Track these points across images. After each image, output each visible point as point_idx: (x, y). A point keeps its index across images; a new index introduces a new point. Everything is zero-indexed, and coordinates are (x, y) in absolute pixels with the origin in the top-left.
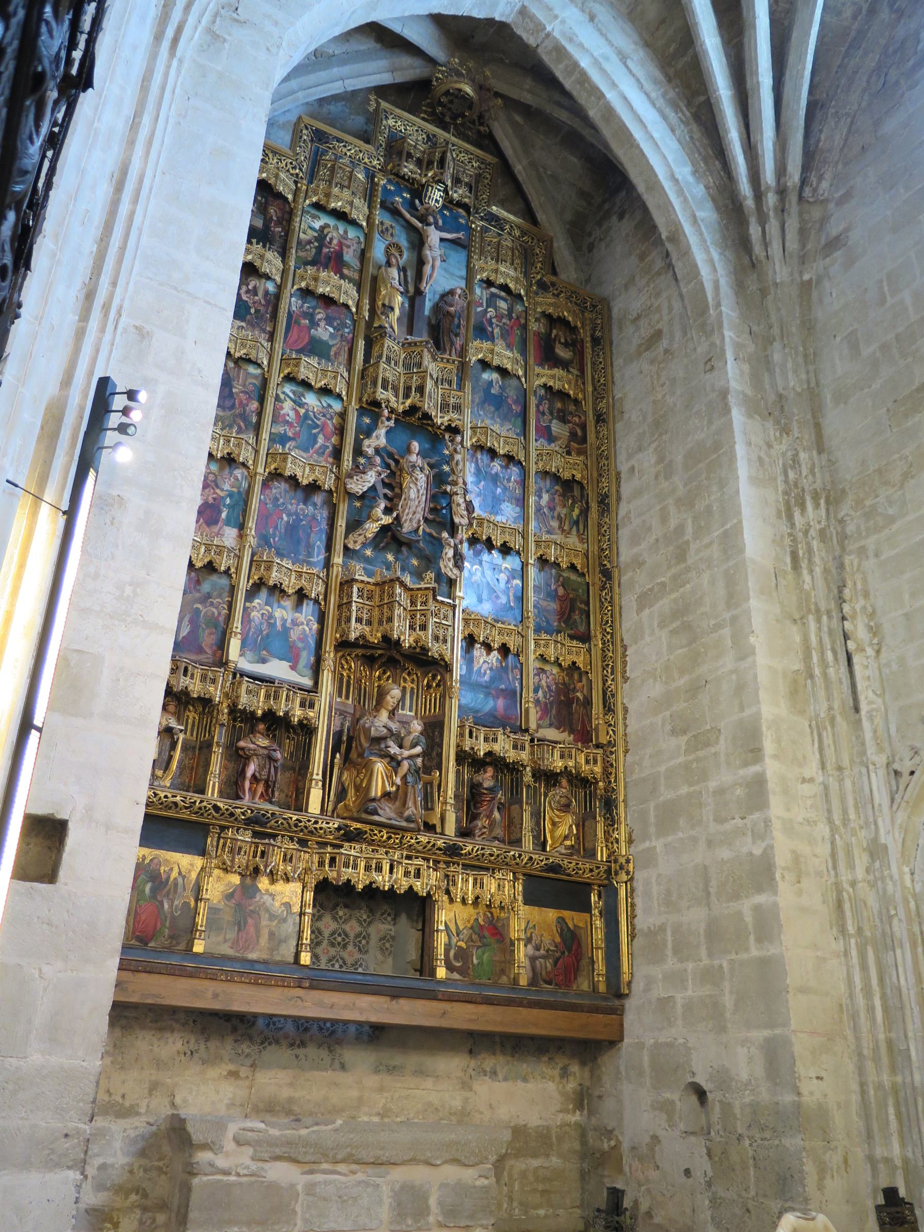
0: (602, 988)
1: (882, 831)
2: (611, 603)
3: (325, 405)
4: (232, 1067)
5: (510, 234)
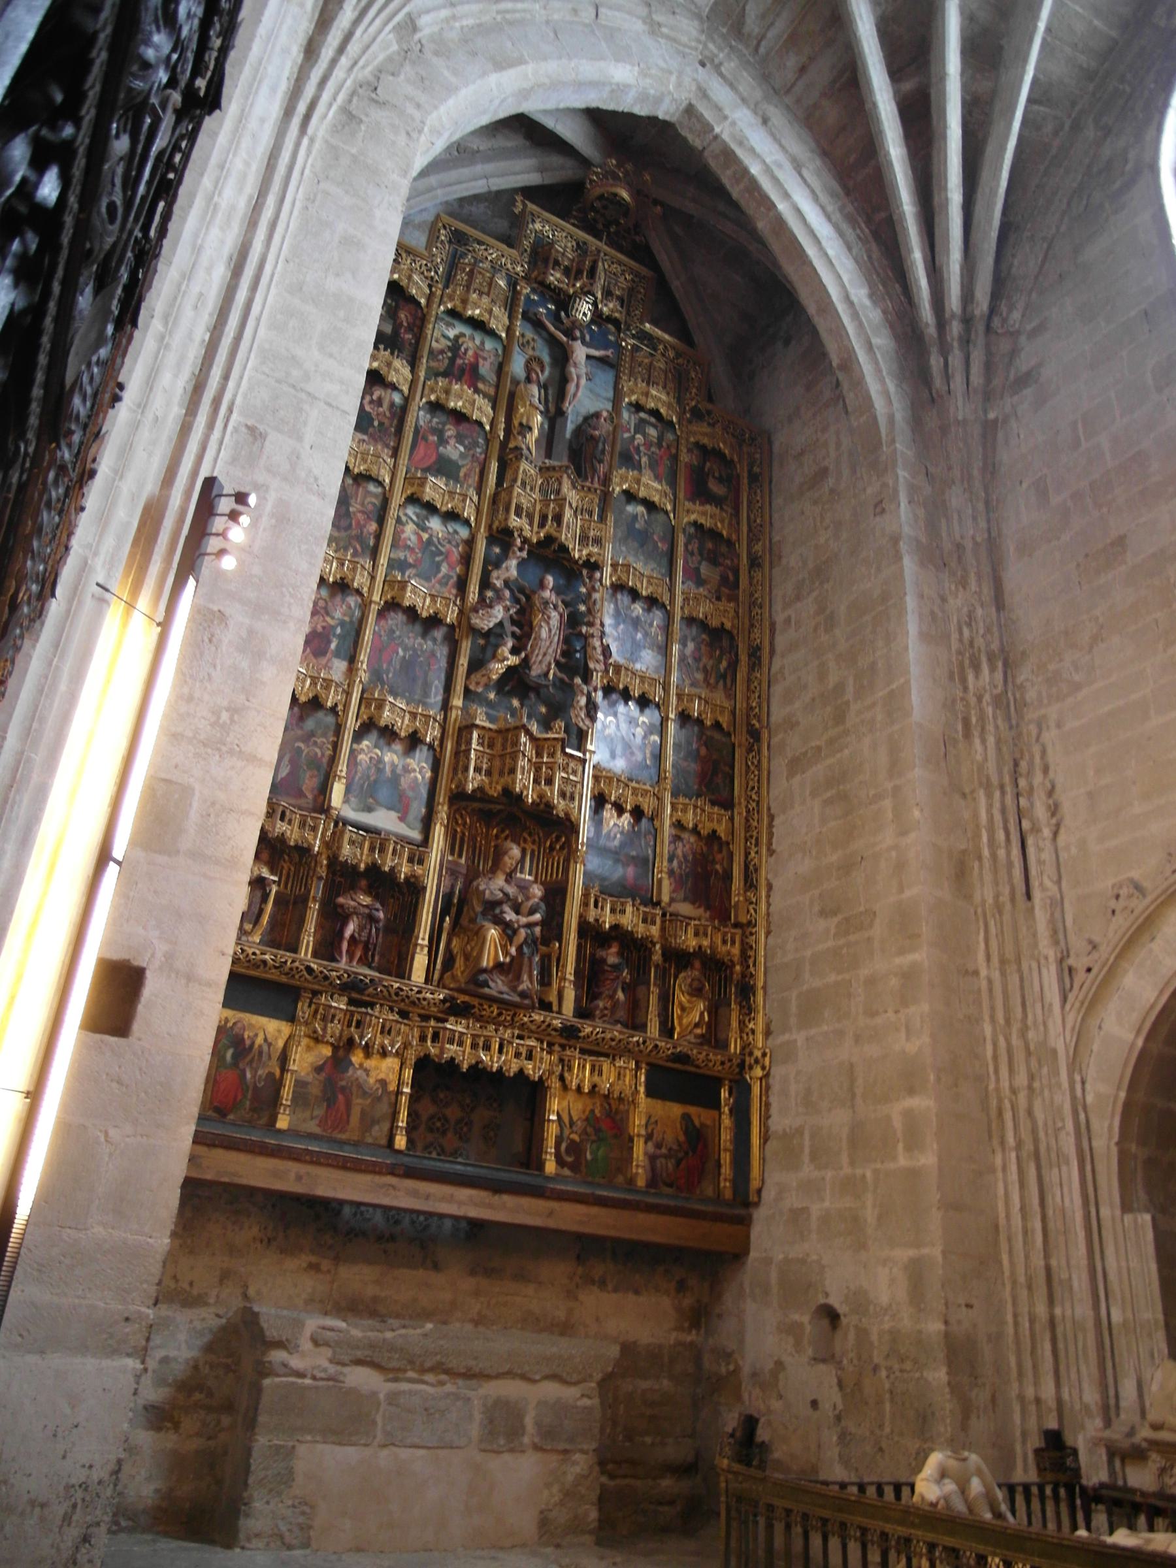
0: (728, 1194)
1: (1052, 1032)
2: (758, 766)
3: (451, 530)
4: (313, 1259)
5: (663, 355)
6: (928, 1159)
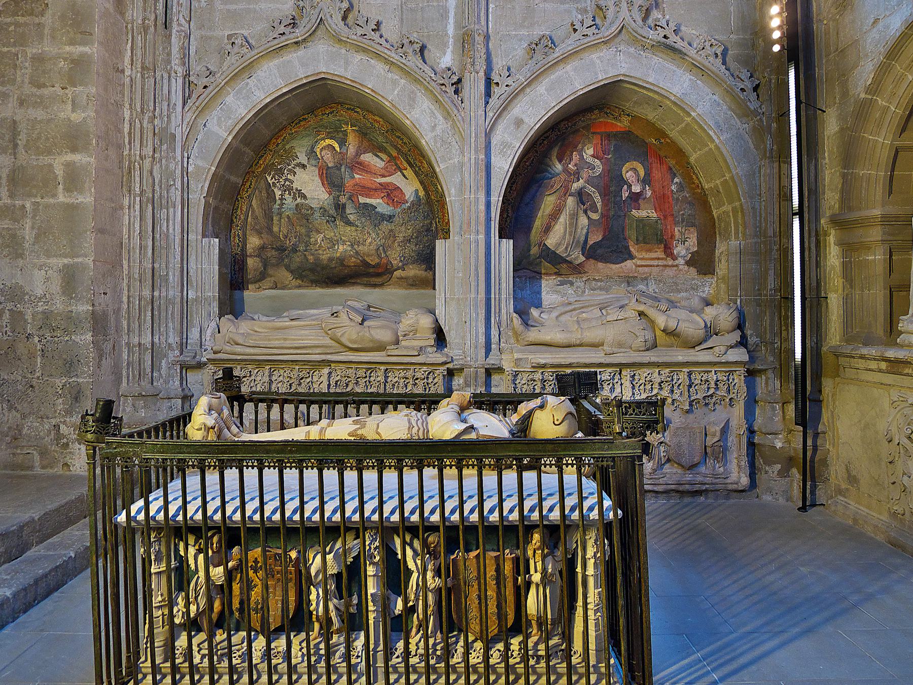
1: (173, 124)
6: (87, 199)
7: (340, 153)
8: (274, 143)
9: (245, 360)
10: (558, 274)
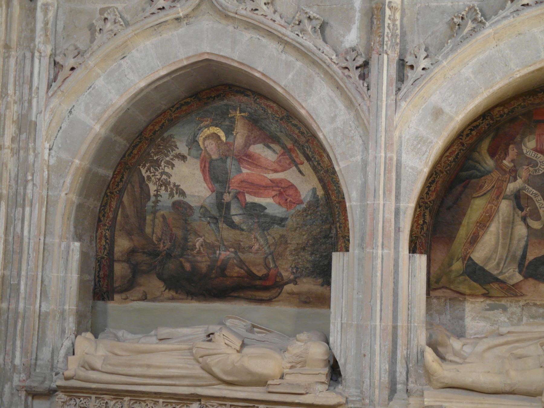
7: (226, 143)
8: (151, 130)
9: (101, 390)
10: (487, 295)
